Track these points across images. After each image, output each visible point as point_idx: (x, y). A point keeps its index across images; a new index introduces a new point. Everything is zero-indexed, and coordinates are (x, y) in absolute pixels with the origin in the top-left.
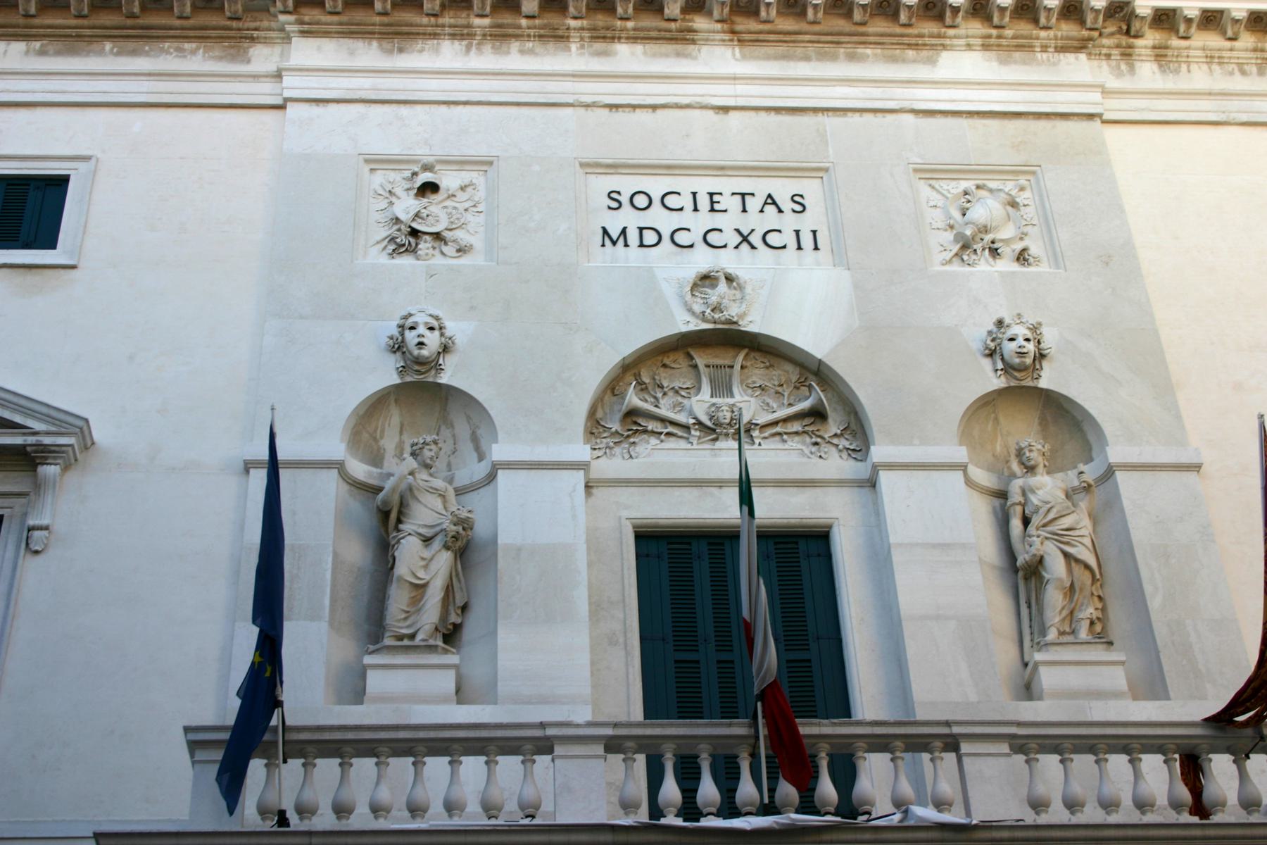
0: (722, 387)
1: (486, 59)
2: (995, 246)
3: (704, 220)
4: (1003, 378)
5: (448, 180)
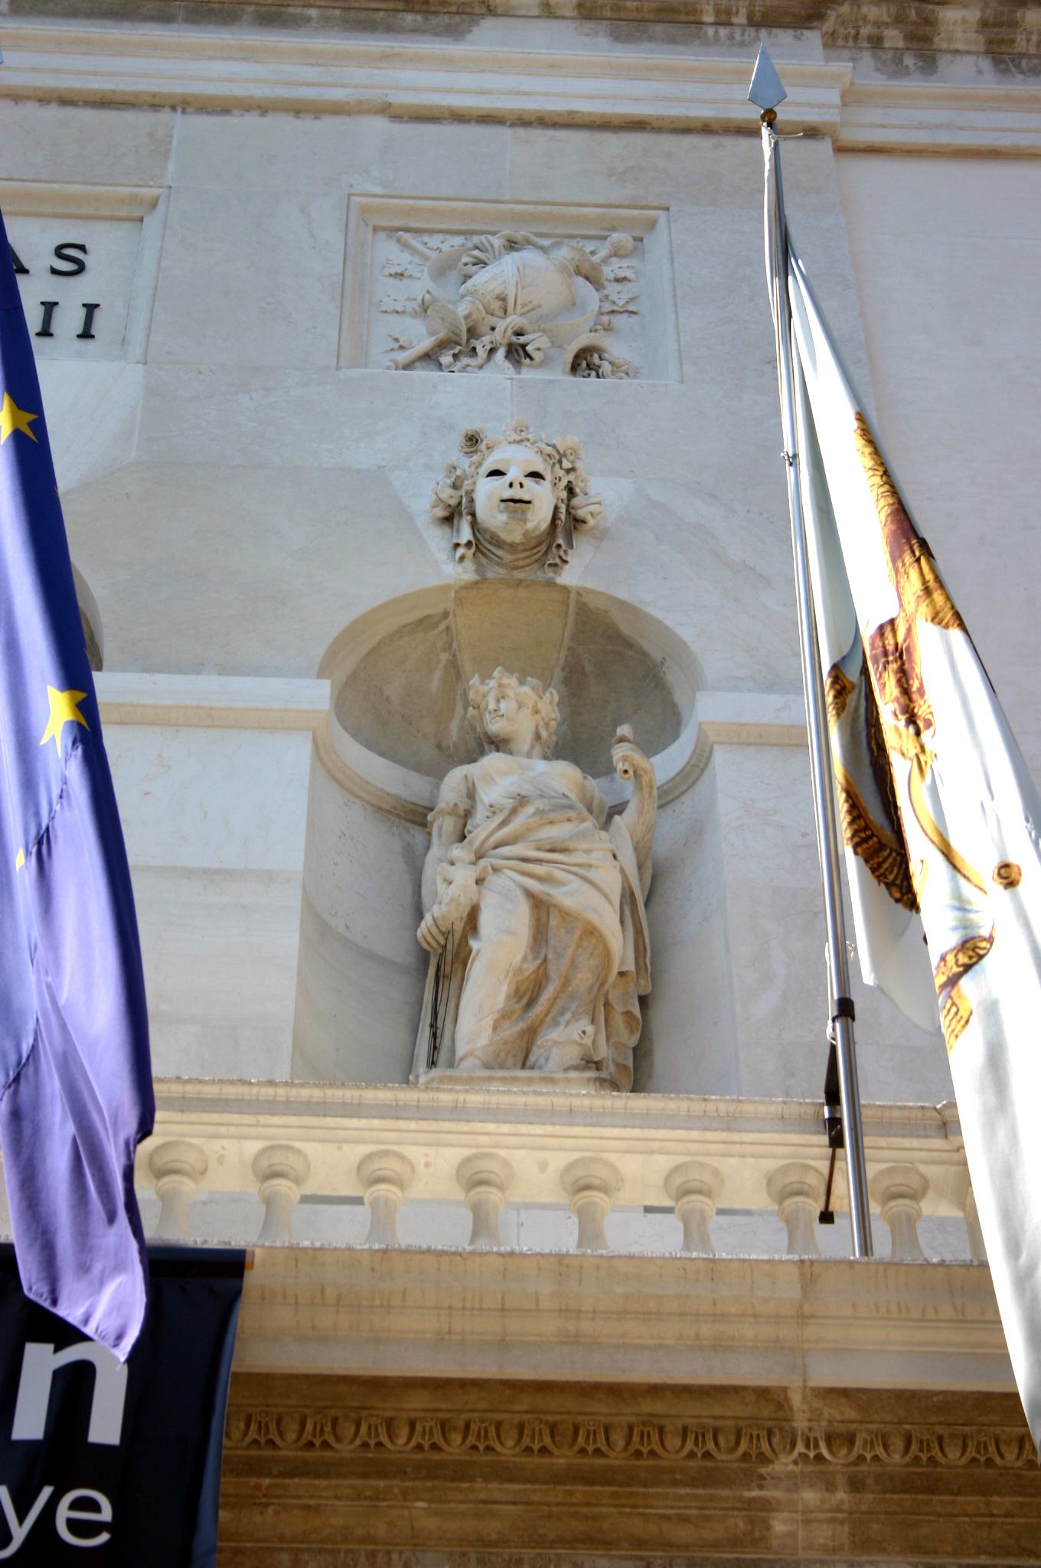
2: (522, 340)
4: (469, 564)
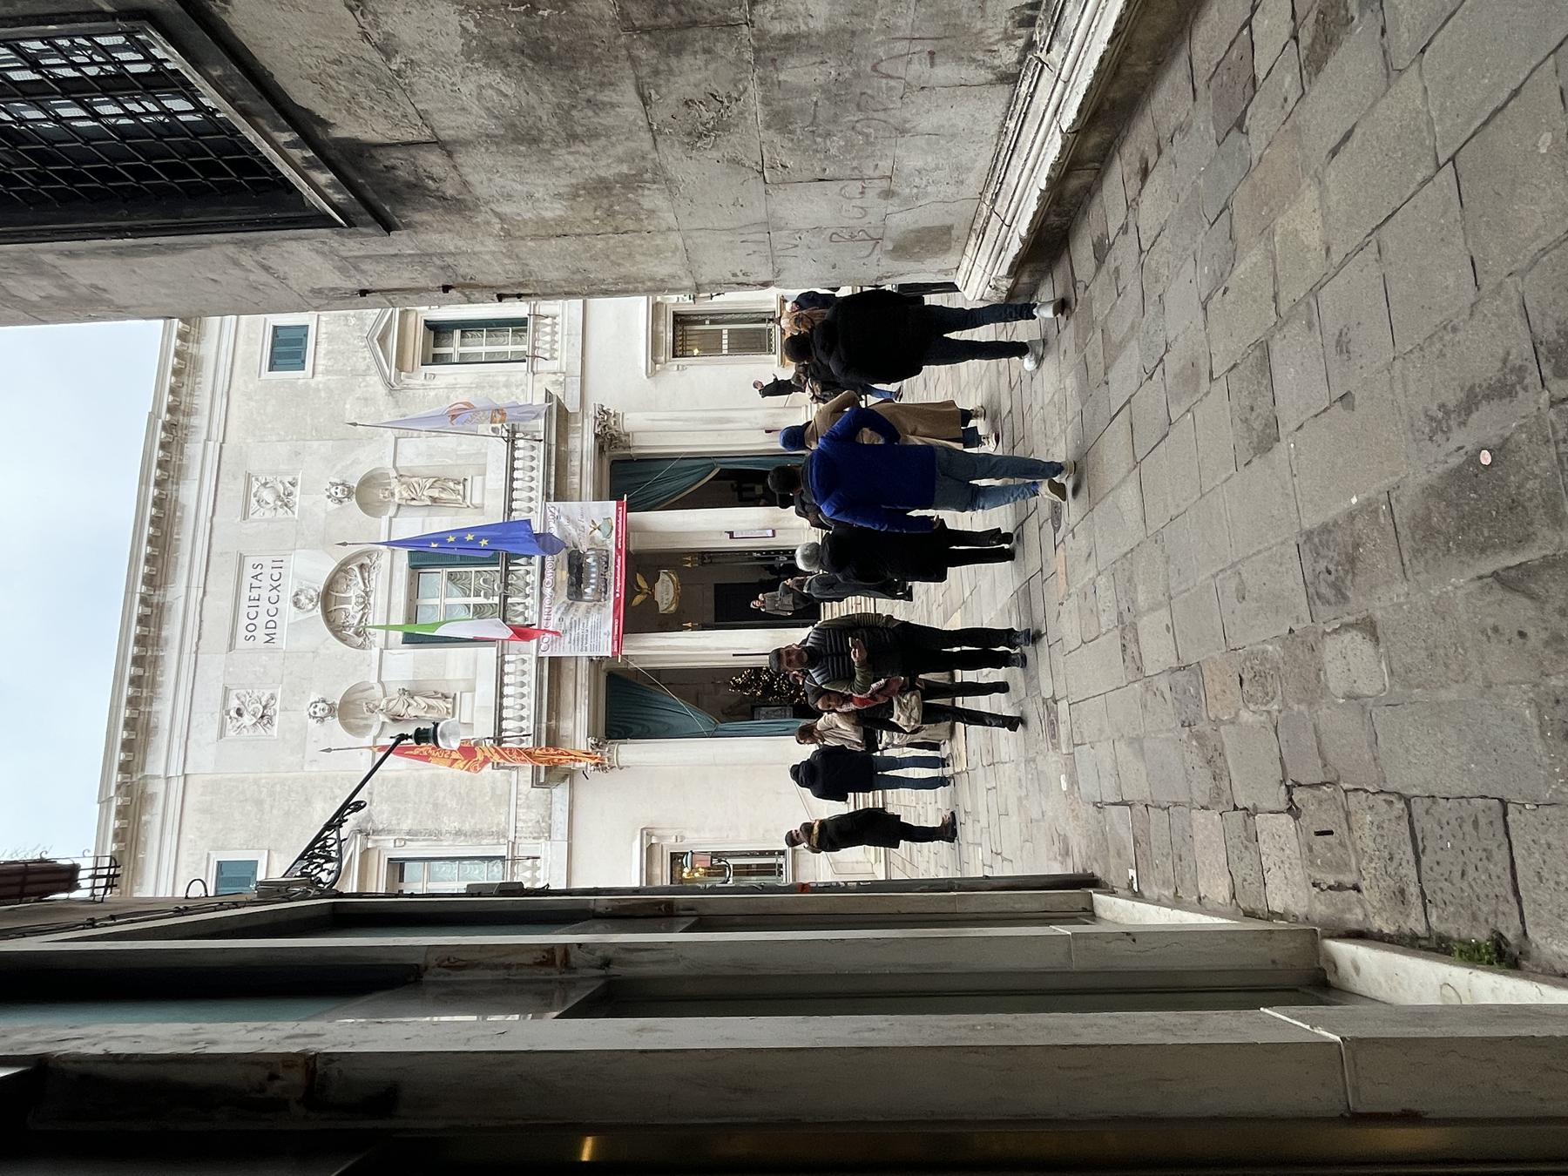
0: (347, 600)
1: (167, 690)
3: (264, 604)
5: (234, 704)
